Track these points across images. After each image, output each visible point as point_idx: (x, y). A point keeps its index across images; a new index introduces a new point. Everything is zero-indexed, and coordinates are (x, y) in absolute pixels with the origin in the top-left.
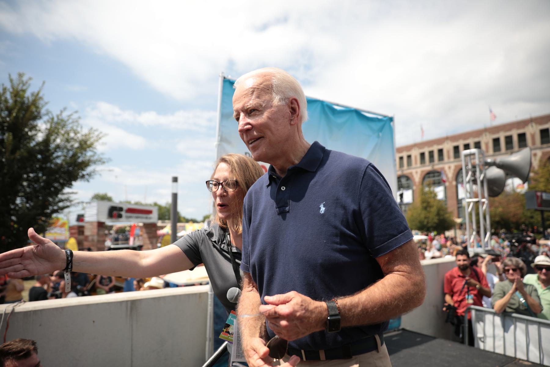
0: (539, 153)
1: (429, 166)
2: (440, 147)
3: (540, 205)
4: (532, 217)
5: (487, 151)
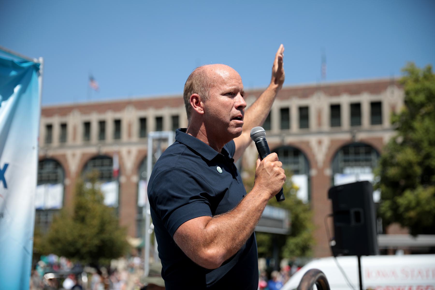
2: (118, 116)
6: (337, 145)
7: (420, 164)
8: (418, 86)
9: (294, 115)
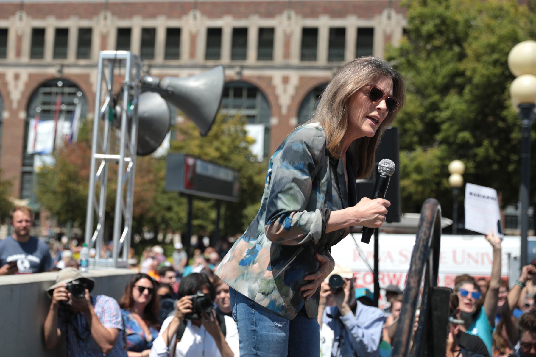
4: (169, 209)
7: (422, 117)
8: (426, 10)
9: (253, 37)
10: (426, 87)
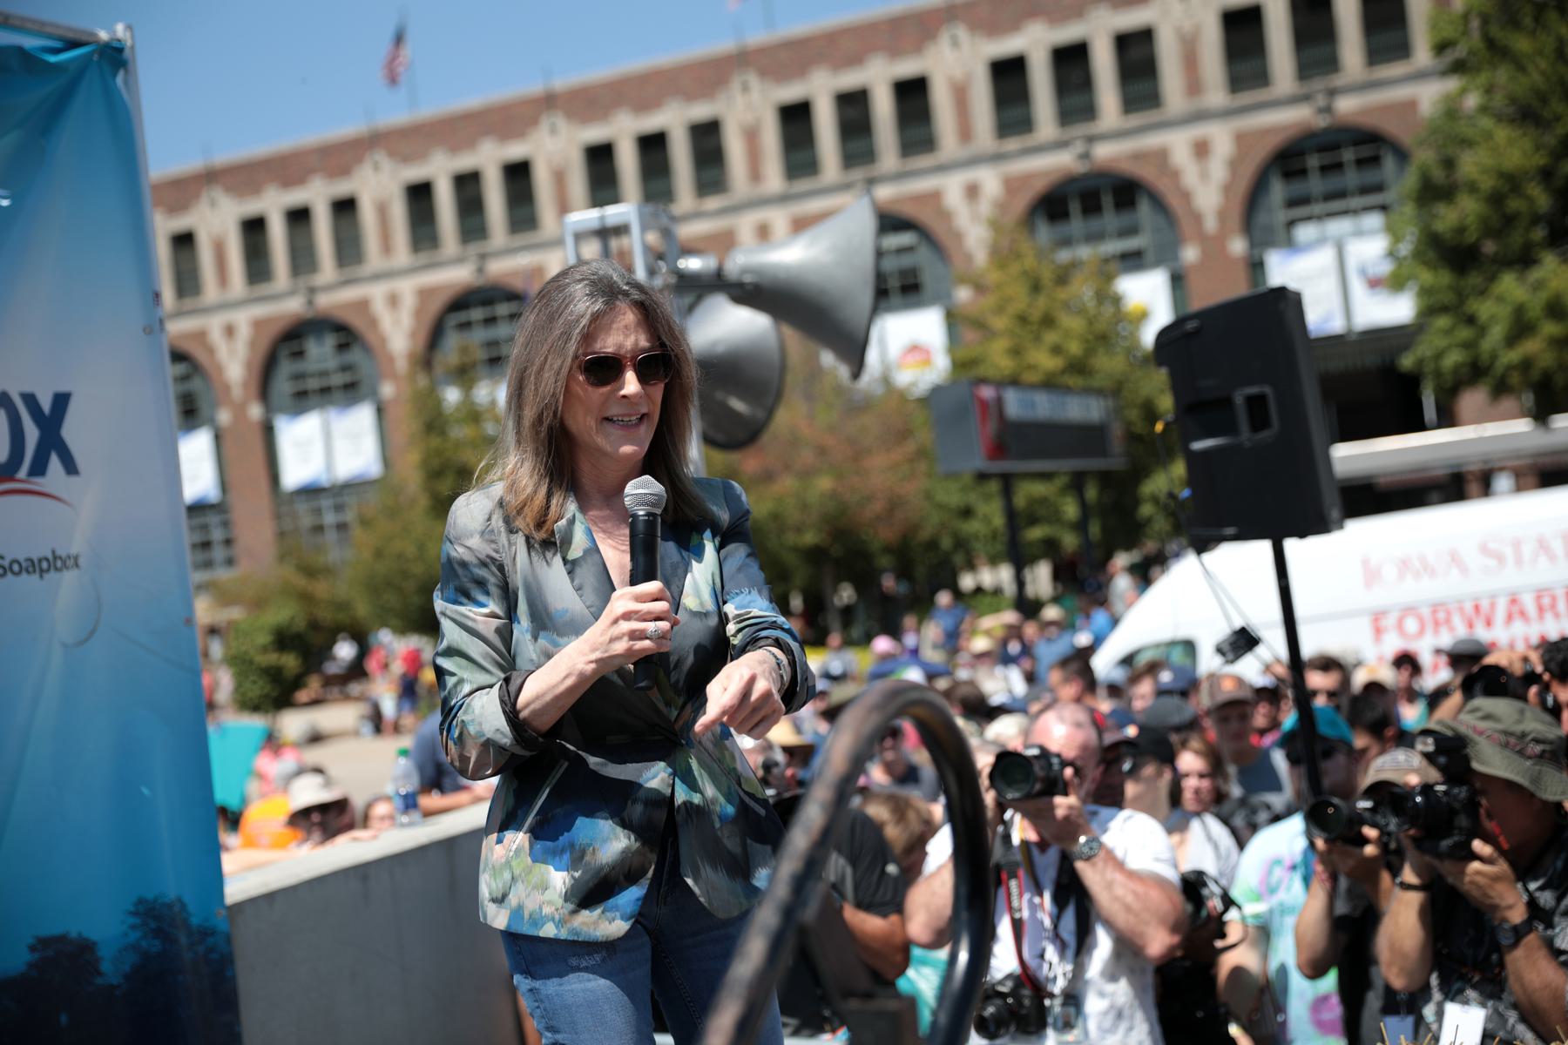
0: (990, 180)
1: (459, 260)
2: (515, 151)
3: (999, 449)
4: (967, 513)
5: (755, 175)
6: (1262, 151)
10: (1543, 99)
